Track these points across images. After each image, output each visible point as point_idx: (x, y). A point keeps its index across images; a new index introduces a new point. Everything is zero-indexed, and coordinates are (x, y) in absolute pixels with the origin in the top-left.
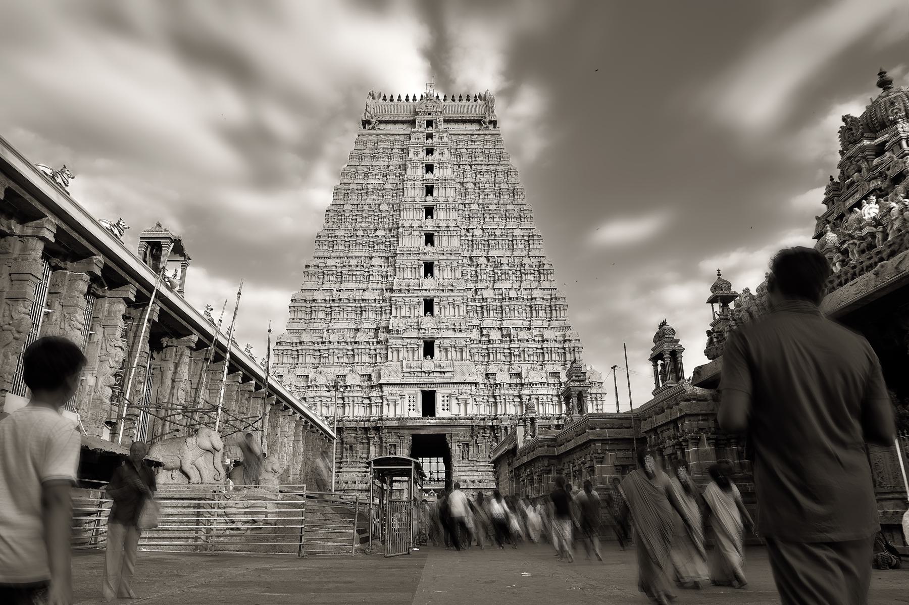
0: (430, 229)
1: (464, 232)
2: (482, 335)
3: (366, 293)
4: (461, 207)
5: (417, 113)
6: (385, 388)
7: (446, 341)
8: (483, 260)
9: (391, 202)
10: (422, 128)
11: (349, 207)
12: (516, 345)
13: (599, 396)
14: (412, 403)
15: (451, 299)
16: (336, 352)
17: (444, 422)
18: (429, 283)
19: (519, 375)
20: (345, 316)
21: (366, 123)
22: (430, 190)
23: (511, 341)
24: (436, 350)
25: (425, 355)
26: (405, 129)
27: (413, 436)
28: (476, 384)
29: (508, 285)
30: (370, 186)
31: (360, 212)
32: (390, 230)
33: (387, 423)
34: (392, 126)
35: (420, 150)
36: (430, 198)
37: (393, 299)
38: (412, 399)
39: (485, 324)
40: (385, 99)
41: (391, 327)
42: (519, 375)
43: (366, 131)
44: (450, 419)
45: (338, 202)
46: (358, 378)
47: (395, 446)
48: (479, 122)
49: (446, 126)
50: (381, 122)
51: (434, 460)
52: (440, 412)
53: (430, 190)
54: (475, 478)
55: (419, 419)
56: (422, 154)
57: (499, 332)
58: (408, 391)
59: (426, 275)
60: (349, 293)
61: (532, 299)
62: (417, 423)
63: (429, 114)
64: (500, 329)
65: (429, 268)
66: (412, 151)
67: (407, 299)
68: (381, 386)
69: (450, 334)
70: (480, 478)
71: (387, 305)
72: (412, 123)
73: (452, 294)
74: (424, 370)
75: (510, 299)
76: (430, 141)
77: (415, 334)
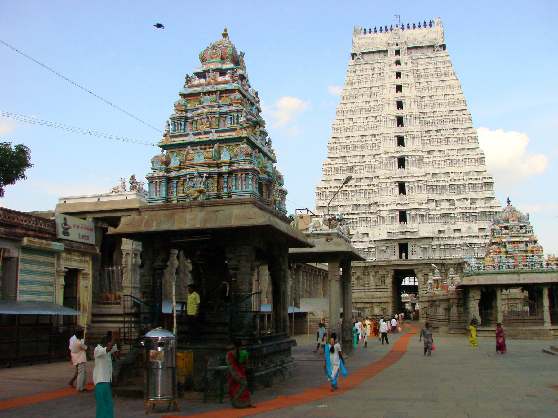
3: (362, 181)
4: (422, 115)
7: (413, 211)
8: (436, 154)
11: (348, 121)
17: (414, 262)
21: (353, 55)
24: (408, 217)
25: (400, 221)
28: (432, 238)
33: (380, 263)
36: (400, 111)
40: (365, 33)
41: (379, 204)
44: (416, 260)
45: (340, 118)
46: (360, 236)
47: (384, 276)
49: (409, 51)
50: (363, 53)
52: (411, 256)
55: (398, 261)
57: (448, 203)
63: (397, 45)
65: (401, 162)
66: (386, 75)
67: (388, 184)
69: (416, 206)
75: (455, 180)
76: (398, 67)
77: (395, 207)
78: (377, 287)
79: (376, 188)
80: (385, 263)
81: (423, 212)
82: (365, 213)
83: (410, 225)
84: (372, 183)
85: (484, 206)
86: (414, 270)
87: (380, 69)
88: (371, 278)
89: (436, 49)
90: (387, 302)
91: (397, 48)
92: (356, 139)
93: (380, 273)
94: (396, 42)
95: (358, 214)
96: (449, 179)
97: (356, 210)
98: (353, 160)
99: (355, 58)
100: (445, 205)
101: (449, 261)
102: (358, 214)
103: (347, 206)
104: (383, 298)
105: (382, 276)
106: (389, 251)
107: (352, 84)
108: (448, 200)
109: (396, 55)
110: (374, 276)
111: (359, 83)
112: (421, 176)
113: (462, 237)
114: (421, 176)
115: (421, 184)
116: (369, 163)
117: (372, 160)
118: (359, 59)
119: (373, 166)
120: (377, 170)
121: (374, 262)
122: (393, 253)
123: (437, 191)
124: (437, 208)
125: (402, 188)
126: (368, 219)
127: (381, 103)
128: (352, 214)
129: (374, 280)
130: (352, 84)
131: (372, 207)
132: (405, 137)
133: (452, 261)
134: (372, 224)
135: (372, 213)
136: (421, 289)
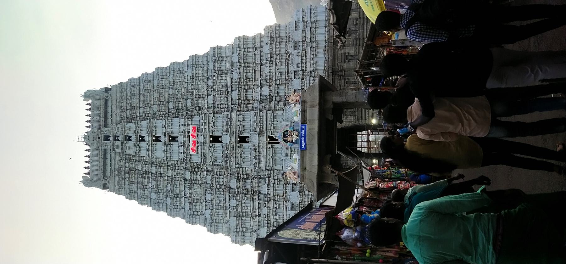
10: (109, 145)
13: (312, 11)
15: (238, 123)
18: (226, 139)
42: (295, 72)
48: (106, 101)
51: (359, 138)
56: (130, 144)
63: (99, 138)
72: (105, 151)
76: (120, 138)
99: (108, 185)
109: (109, 140)
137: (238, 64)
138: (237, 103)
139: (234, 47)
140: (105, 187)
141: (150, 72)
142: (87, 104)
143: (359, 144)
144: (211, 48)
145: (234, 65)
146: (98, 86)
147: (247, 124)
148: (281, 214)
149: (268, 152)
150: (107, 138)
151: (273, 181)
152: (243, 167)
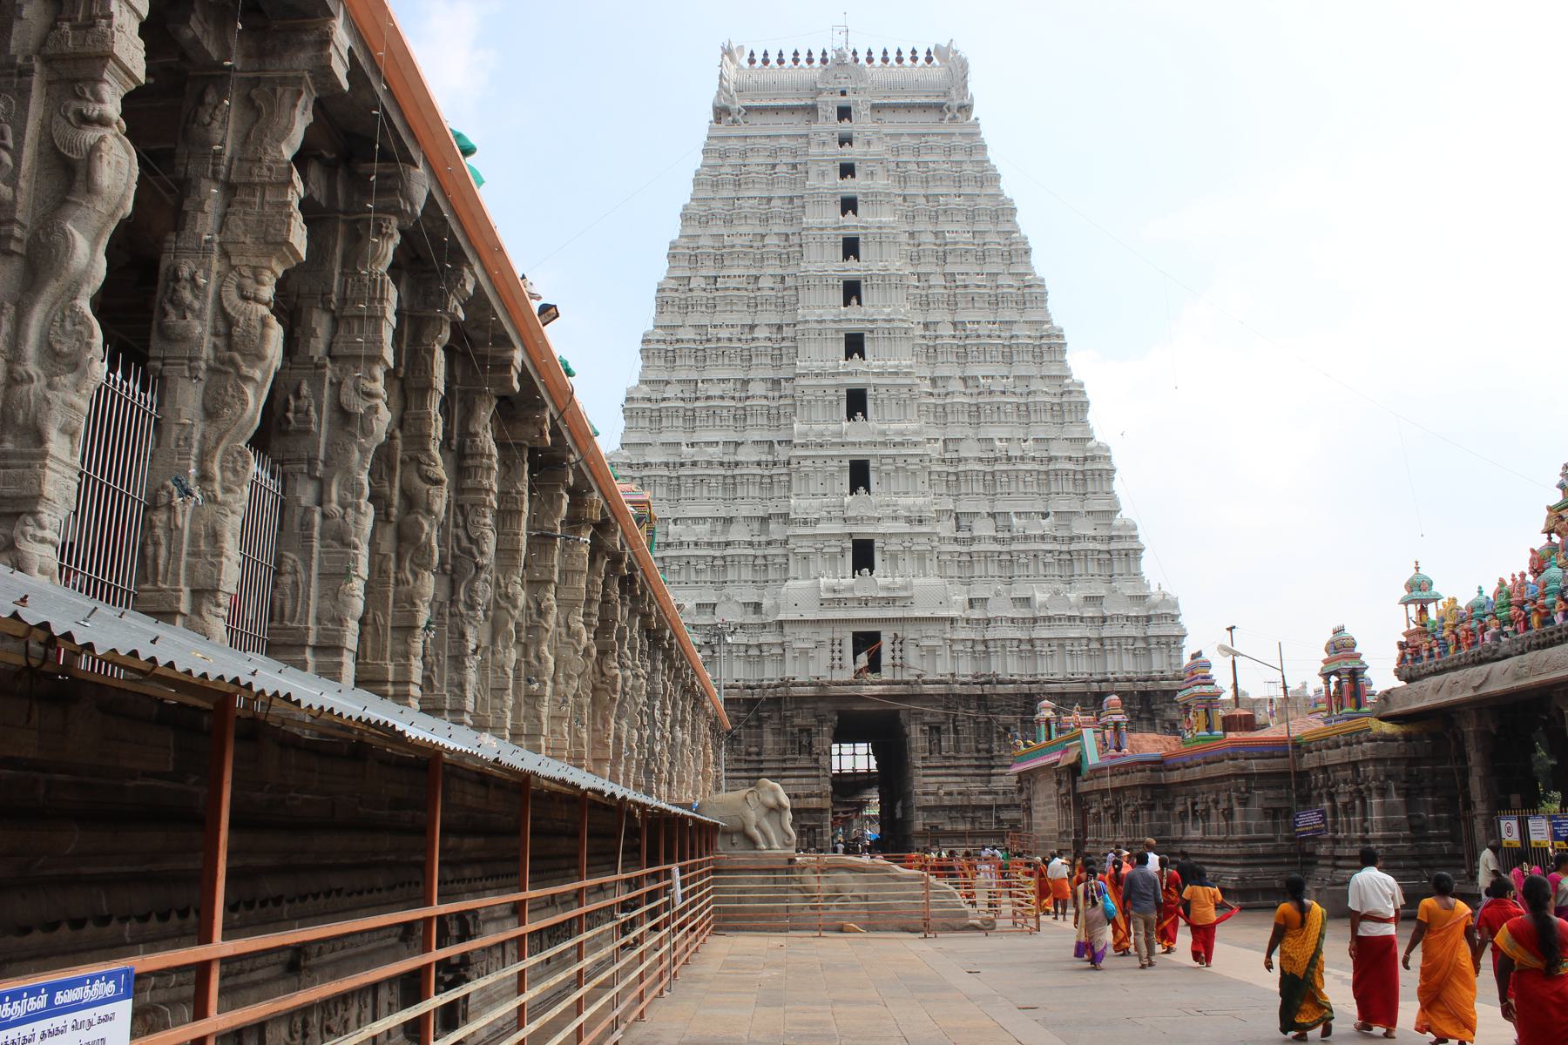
0: (855, 327)
1: (919, 331)
2: (958, 528)
5: (820, 92)
6: (787, 629)
7: (894, 540)
8: (956, 386)
9: (779, 271)
12: (1022, 547)
14: (837, 655)
15: (900, 463)
16: (693, 562)
17: (898, 690)
19: (1026, 601)
20: (705, 494)
22: (851, 248)
23: (1013, 539)
24: (878, 557)
26: (797, 125)
27: (839, 713)
28: (952, 620)
29: (1004, 432)
30: (738, 241)
31: (720, 293)
32: (780, 327)
33: (796, 692)
34: (771, 118)
35: (830, 167)
37: (794, 461)
38: (837, 648)
39: (964, 506)
40: (752, 61)
41: (792, 516)
43: (723, 130)
45: (678, 273)
46: (738, 610)
47: (808, 731)
50: (749, 109)
53: (851, 248)
54: (955, 788)
58: (825, 635)
59: (851, 415)
60: (710, 450)
61: (1050, 459)
62: (850, 691)
63: (843, 93)
64: (993, 515)
65: (856, 402)
68: (781, 624)
69: (902, 527)
70: (963, 788)
71: (779, 472)
73: (904, 452)
74: (858, 594)
75: (1009, 459)
77: (837, 528)
78: (789, 765)
79: (784, 470)
80: (809, 691)
81: (922, 545)
82: (751, 544)
83: (882, 578)
84: (770, 458)
85: (1093, 533)
86: (897, 711)
87: (795, 154)
88: (769, 739)
89: (949, 115)
90: (821, 811)
91: (843, 101)
92: (724, 334)
93: (797, 721)
94: (843, 87)
95: (727, 544)
96: (991, 455)
97: (723, 532)
98: (715, 391)
100: (984, 528)
101: (1000, 689)
102: (727, 544)
103: (696, 520)
104: (808, 796)
105: (801, 731)
106: (824, 656)
107: (715, 185)
108: (993, 515)
109: (841, 118)
110: (778, 732)
111: (738, 184)
112: (915, 444)
113: (1035, 620)
114: (915, 444)
115: (914, 464)
116: (764, 402)
117: (770, 394)
118: (734, 121)
119: (773, 411)
120: (783, 421)
121: (777, 686)
122: (837, 662)
123: (958, 486)
124: (960, 535)
125: (859, 475)
126: (760, 561)
127: (795, 240)
128: (710, 544)
129: (775, 743)
130: (715, 185)
131: (773, 526)
132: (867, 335)
133: (1010, 688)
134: (772, 575)
135: (769, 543)
136: (922, 772)
137: (1045, 454)
138: (948, 456)
139: (1090, 444)
140: (721, 113)
141: (1018, 219)
142: (929, 52)
143: (847, 748)
144: (1082, 385)
145: (1043, 446)
146: (977, 87)
147: (899, 483)
148: (683, 578)
149: (833, 543)
150: (844, 113)
151: (759, 553)
152: (789, 475)
